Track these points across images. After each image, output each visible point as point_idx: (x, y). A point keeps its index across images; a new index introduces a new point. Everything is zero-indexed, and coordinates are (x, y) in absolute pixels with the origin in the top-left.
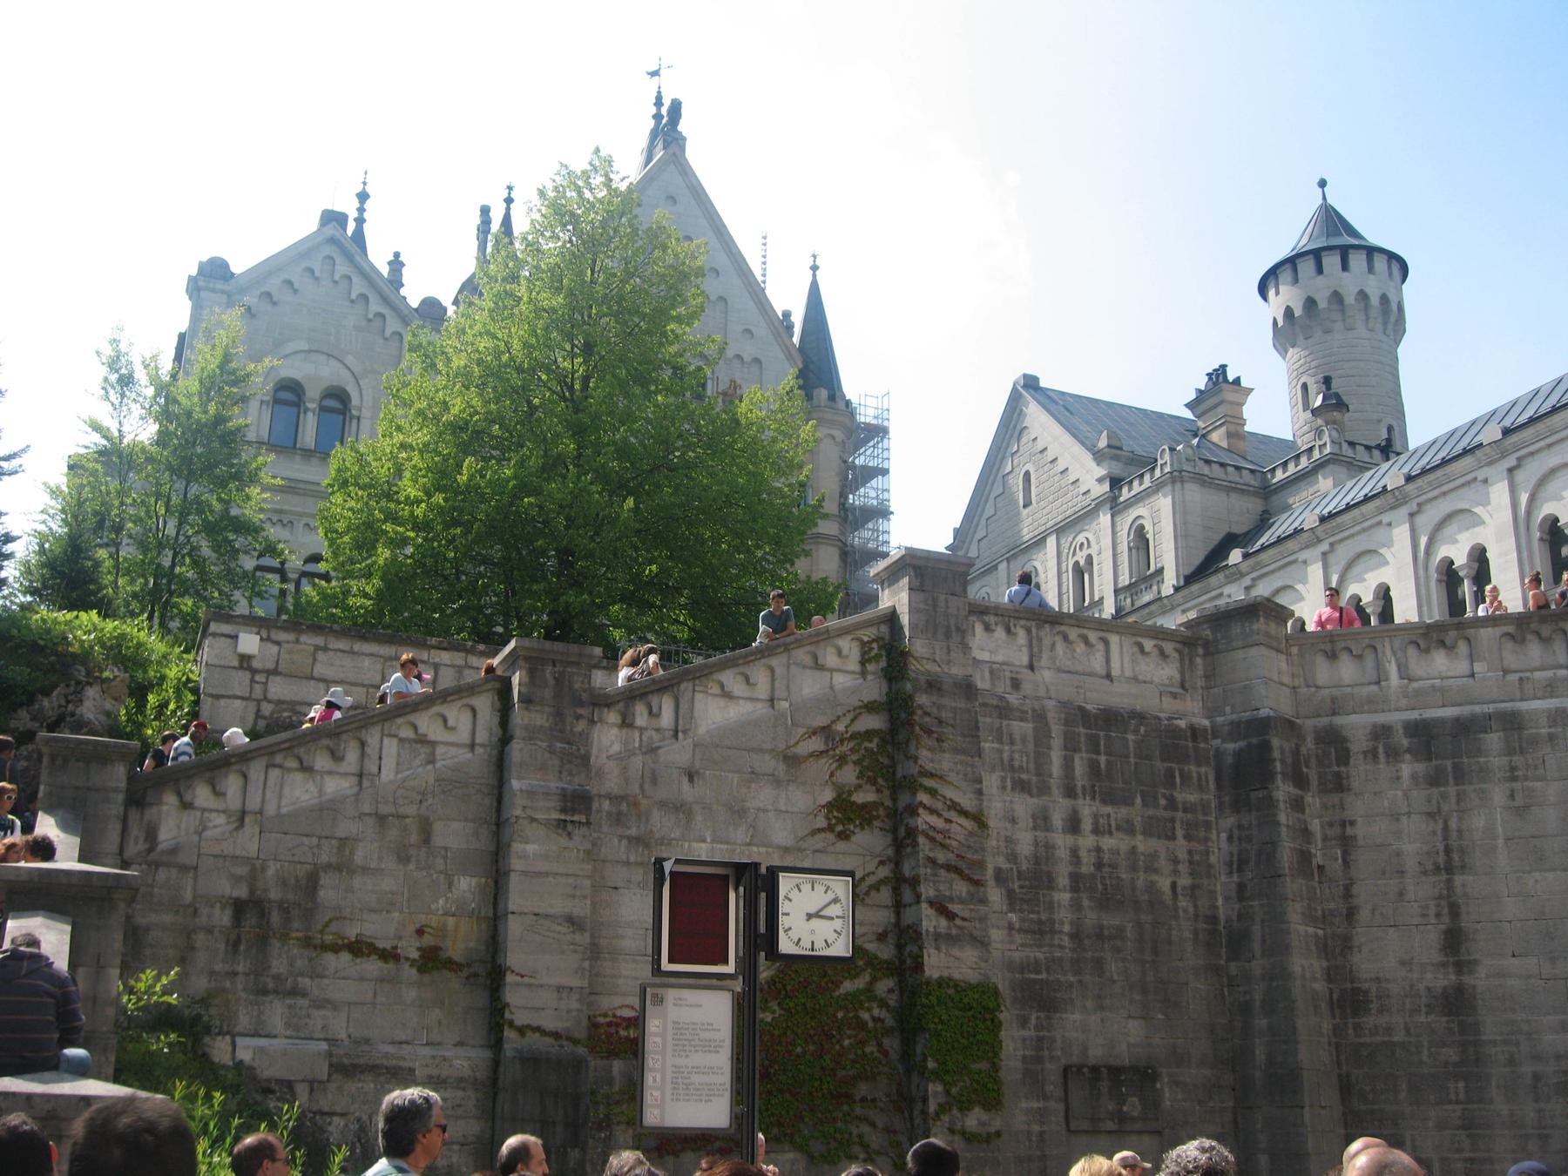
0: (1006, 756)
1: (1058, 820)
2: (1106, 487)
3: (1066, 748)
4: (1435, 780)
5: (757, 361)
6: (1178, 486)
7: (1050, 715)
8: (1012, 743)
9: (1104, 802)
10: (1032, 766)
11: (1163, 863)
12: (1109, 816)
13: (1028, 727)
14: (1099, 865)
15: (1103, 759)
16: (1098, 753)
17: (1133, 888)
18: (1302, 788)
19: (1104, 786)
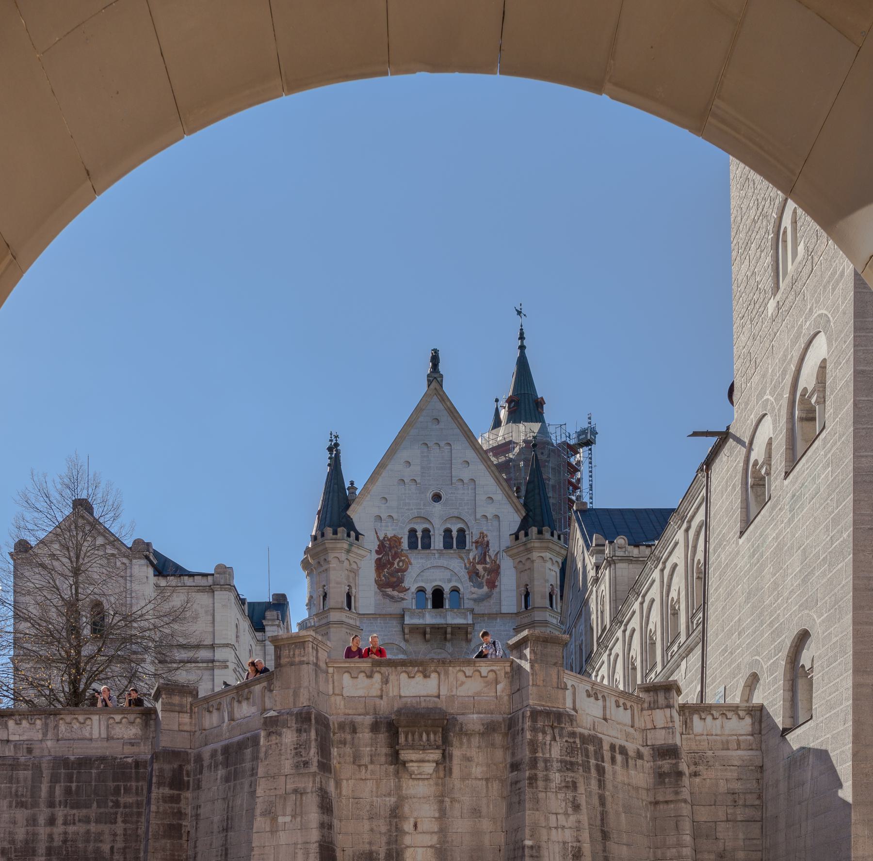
0: (13, 790)
1: (42, 820)
3: (51, 781)
4: (227, 779)
7: (44, 766)
8: (18, 782)
9: (72, 808)
10: (29, 793)
11: (107, 837)
12: (74, 815)
13: (29, 773)
14: (65, 841)
15: (74, 785)
16: (72, 782)
17: (85, 851)
18: (180, 789)
19: (73, 800)
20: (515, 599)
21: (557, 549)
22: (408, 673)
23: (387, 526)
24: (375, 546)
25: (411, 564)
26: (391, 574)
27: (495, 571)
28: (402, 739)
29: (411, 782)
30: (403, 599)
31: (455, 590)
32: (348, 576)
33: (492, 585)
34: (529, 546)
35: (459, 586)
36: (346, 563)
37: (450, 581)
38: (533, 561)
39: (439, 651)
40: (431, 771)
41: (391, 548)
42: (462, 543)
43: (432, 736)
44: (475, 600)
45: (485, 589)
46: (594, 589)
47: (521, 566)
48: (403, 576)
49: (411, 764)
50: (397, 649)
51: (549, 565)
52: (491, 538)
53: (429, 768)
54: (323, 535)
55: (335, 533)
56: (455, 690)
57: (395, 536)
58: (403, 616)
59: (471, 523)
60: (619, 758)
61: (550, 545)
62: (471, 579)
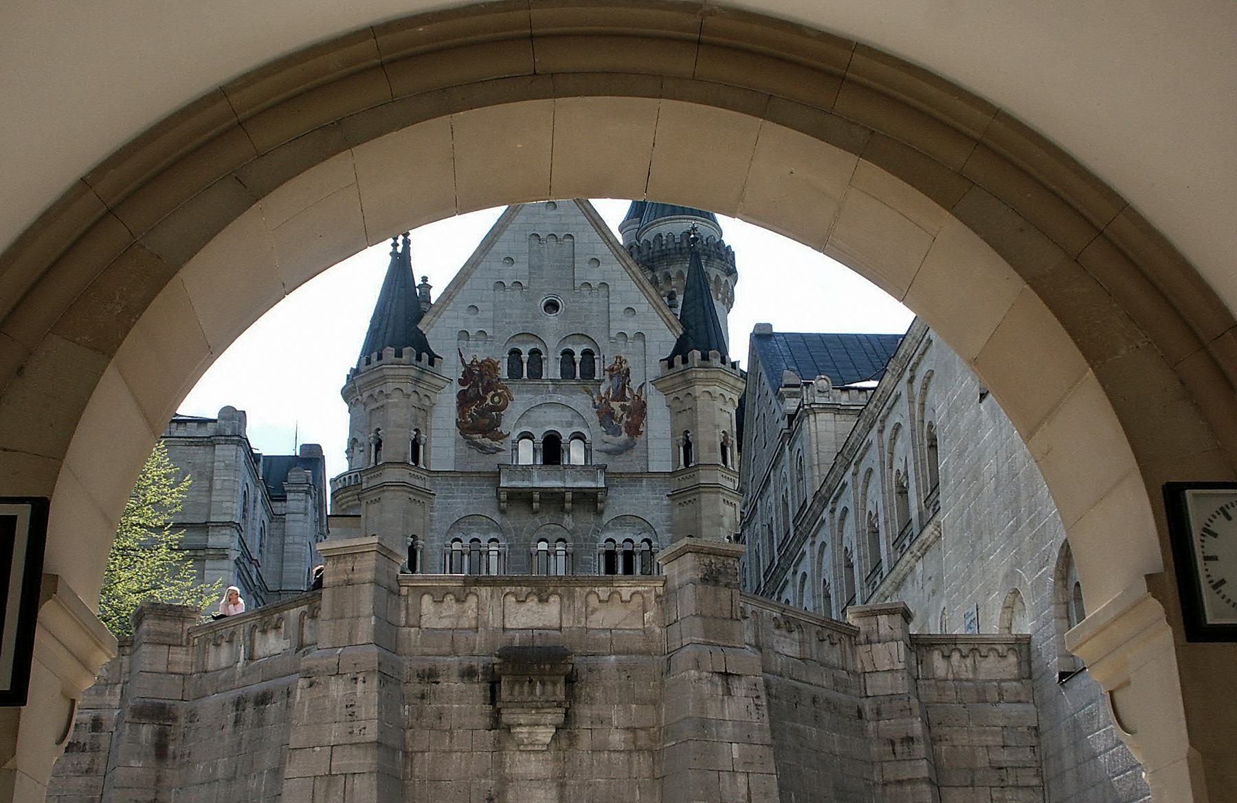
2: (784, 424)
5: (640, 335)
6: (812, 417)
21: (732, 381)
22: (515, 595)
23: (477, 345)
26: (482, 414)
28: (504, 693)
29: (518, 757)
30: (499, 450)
32: (416, 416)
33: (634, 430)
35: (585, 432)
36: (414, 397)
37: (570, 424)
38: (695, 398)
39: (553, 527)
40: (548, 740)
41: (481, 376)
43: (549, 688)
44: (608, 452)
45: (624, 436)
46: (787, 448)
47: (677, 404)
48: (499, 416)
49: (518, 730)
50: (488, 524)
51: (719, 404)
52: (633, 363)
53: (545, 735)
54: (380, 357)
55: (399, 354)
56: (583, 620)
58: (496, 476)
60: (827, 717)
61: (721, 376)
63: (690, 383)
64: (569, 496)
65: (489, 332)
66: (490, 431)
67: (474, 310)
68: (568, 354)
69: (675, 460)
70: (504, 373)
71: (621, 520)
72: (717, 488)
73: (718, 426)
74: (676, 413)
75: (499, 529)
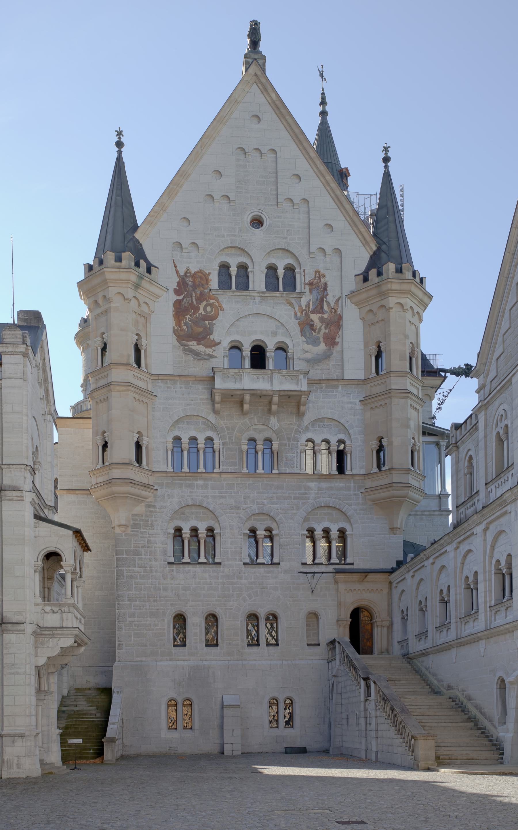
20: (362, 361)
21: (420, 294)
24: (173, 283)
25: (222, 310)
26: (196, 323)
27: (336, 323)
30: (211, 356)
31: (282, 348)
34: (384, 288)
37: (274, 334)
38: (388, 310)
39: (261, 427)
41: (195, 286)
42: (291, 283)
44: (308, 361)
50: (204, 423)
51: (409, 315)
57: (200, 271)
59: (303, 257)
61: (413, 289)
62: (303, 333)
63: (384, 295)
64: (276, 398)
65: (200, 243)
66: (204, 338)
67: (185, 223)
68: (272, 269)
69: (367, 368)
70: (214, 283)
71: (320, 421)
72: (406, 393)
73: (406, 337)
74: (369, 325)
75: (214, 428)
